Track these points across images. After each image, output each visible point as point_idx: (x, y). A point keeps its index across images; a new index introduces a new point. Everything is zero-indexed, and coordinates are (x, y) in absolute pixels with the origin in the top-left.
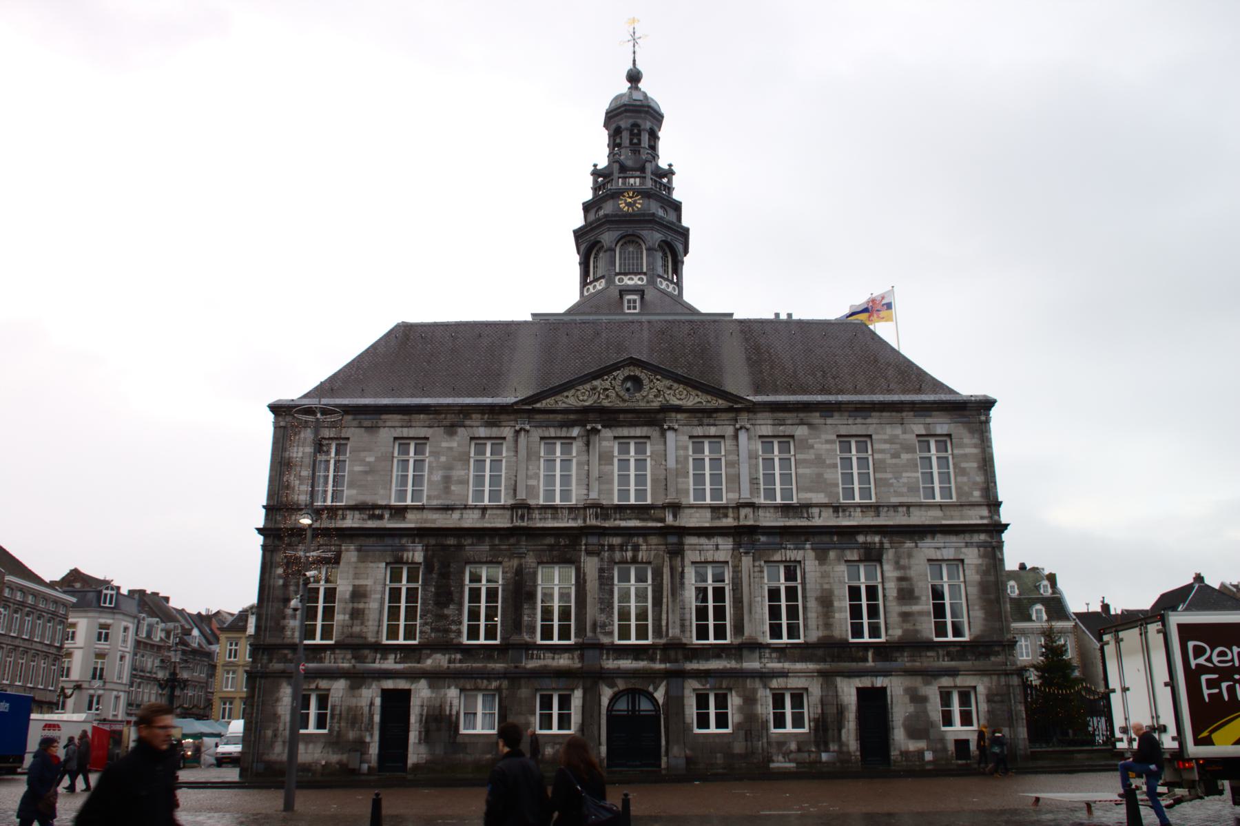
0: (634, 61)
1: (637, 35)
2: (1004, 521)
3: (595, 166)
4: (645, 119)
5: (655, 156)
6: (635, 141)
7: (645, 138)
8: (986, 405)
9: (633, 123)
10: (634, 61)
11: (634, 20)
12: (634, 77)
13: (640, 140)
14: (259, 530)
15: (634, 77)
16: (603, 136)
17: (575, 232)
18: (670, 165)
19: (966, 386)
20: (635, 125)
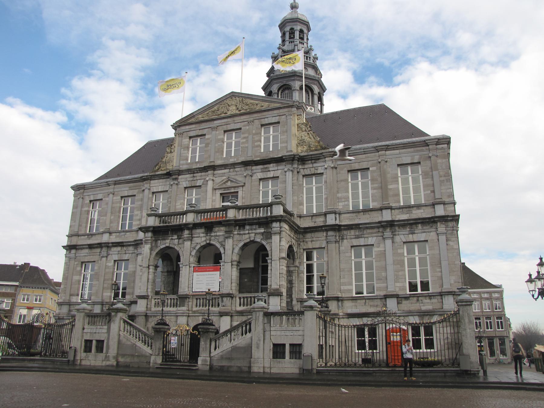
2: (457, 213)
3: (273, 53)
4: (297, 25)
6: (292, 36)
7: (297, 34)
12: (294, 7)
13: (294, 36)
14: (64, 247)
15: (294, 7)
19: (433, 131)
20: (292, 29)
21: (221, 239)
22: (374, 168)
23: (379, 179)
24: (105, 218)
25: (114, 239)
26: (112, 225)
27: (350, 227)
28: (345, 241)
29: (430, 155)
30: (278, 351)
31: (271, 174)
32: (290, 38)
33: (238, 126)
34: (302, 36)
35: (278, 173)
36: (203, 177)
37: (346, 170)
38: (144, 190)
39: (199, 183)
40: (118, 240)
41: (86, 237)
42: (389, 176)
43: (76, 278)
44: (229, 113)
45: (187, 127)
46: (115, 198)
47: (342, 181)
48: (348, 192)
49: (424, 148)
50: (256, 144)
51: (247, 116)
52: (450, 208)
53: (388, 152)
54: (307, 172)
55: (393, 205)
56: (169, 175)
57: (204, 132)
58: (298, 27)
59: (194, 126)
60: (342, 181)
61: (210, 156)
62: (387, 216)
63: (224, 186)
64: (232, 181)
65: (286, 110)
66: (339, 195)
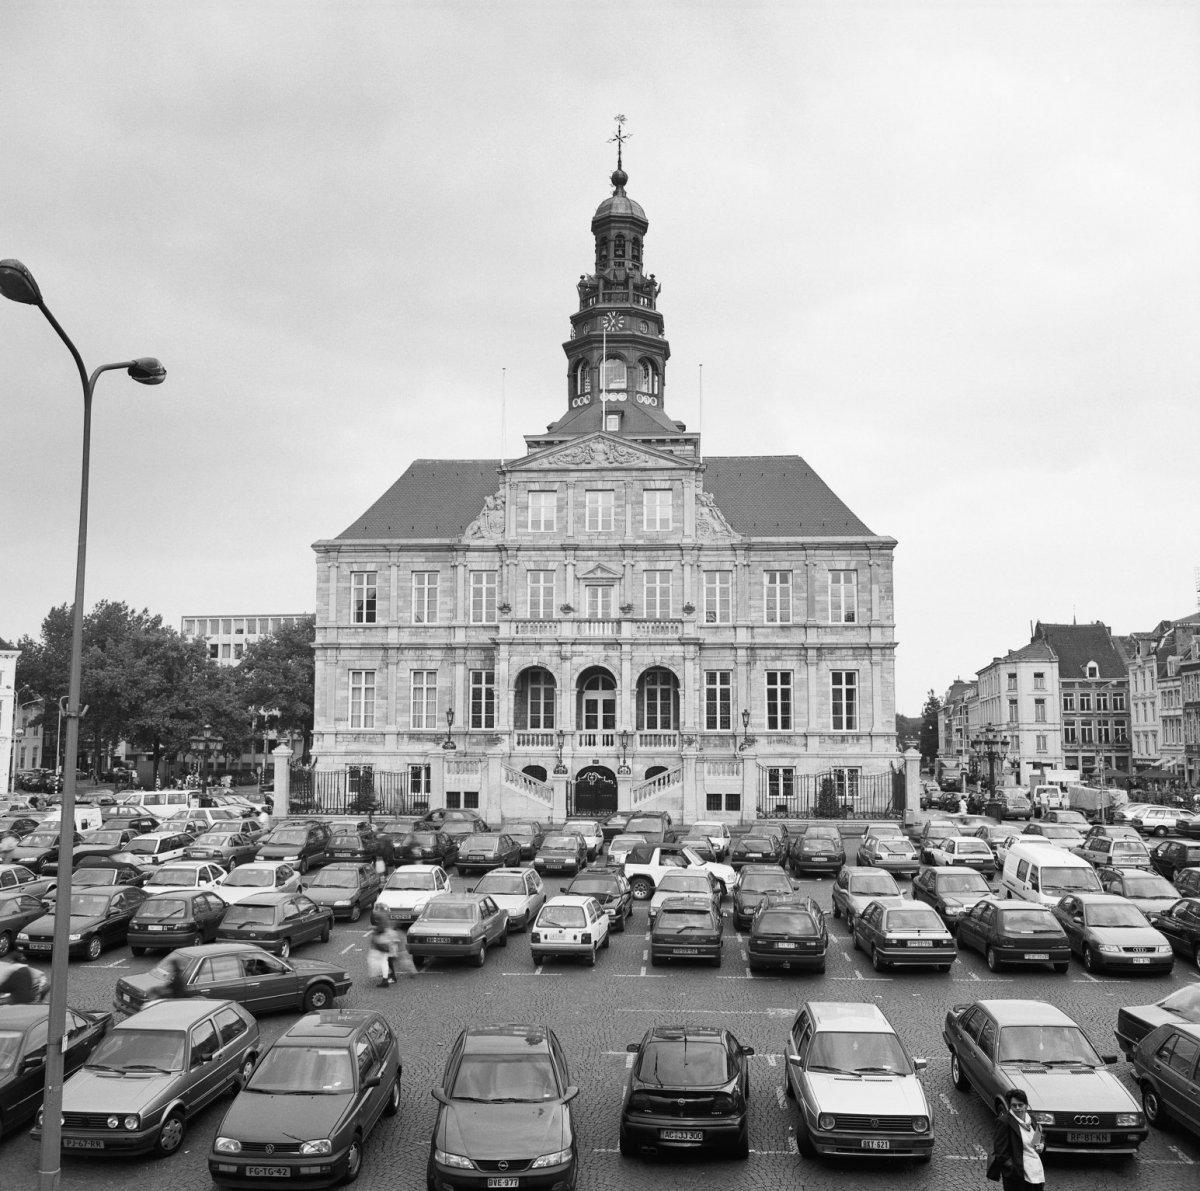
0: (620, 161)
1: (622, 134)
3: (582, 277)
5: (638, 266)
7: (629, 247)
8: (890, 545)
9: (618, 233)
10: (620, 161)
11: (622, 119)
12: (619, 180)
13: (624, 252)
15: (619, 180)
16: (590, 240)
17: (564, 346)
18: (652, 276)
20: (620, 236)
21: (616, 661)
22: (799, 571)
23: (805, 588)
24: (386, 603)
25: (406, 638)
26: (401, 615)
27: (765, 647)
28: (758, 663)
29: (871, 563)
30: (713, 802)
31: (661, 565)
32: (616, 256)
33: (609, 486)
34: (636, 254)
35: (671, 565)
36: (556, 559)
37: (761, 568)
38: (456, 566)
39: (551, 566)
40: (415, 640)
41: (353, 630)
42: (817, 583)
43: (341, 694)
44: (593, 465)
45: (524, 474)
46: (401, 573)
47: (756, 583)
48: (762, 599)
49: (864, 552)
50: (638, 518)
51: (623, 473)
52: (888, 632)
53: (817, 552)
54: (713, 567)
55: (822, 623)
56: (500, 548)
57: (556, 487)
58: (628, 234)
59: (535, 475)
60: (756, 583)
61: (566, 528)
62: (813, 638)
63: (591, 575)
64: (604, 570)
65: (682, 472)
66: (752, 602)
